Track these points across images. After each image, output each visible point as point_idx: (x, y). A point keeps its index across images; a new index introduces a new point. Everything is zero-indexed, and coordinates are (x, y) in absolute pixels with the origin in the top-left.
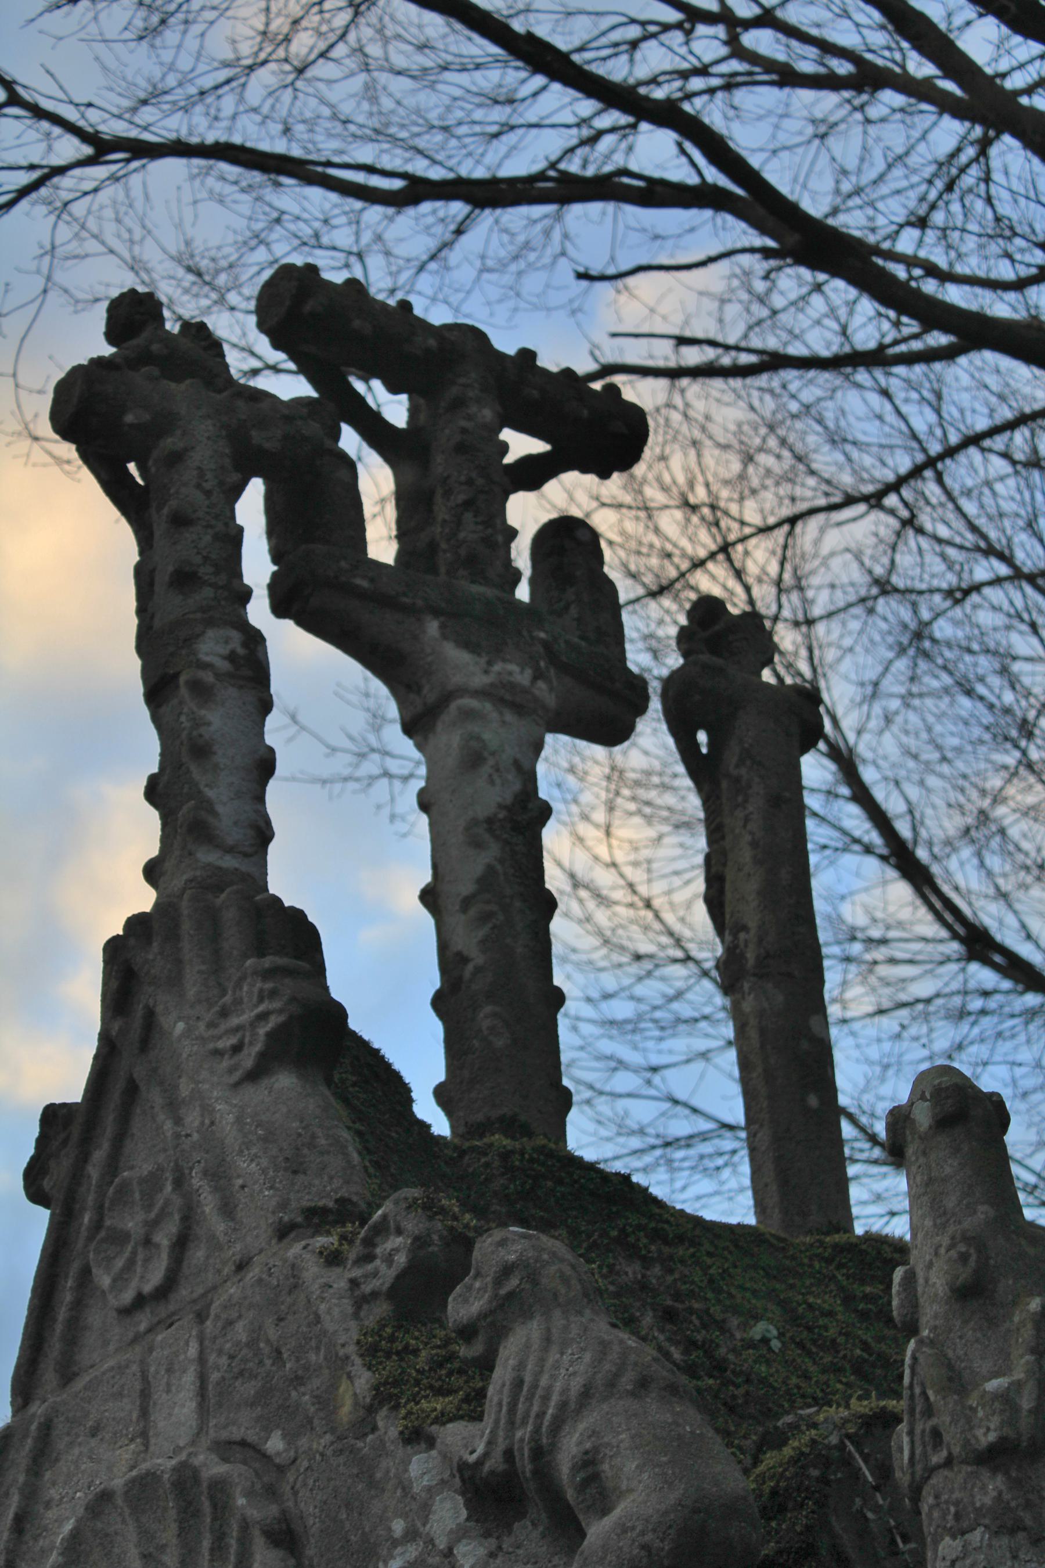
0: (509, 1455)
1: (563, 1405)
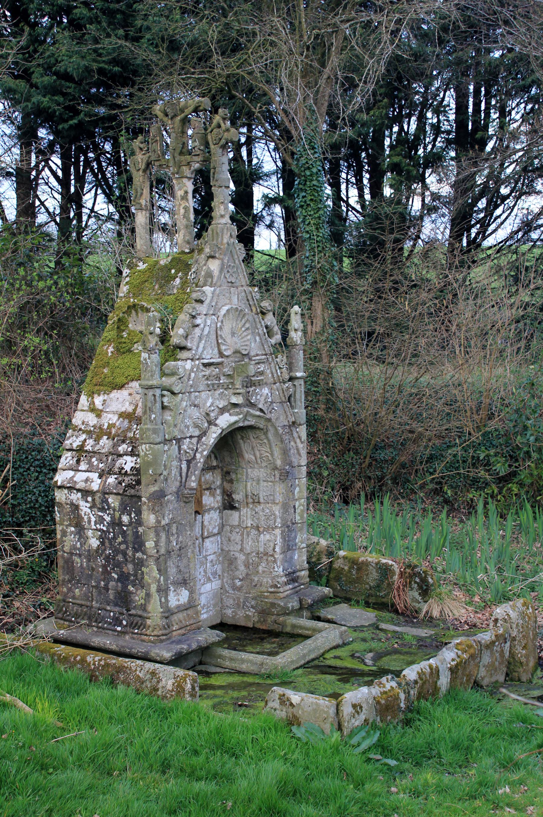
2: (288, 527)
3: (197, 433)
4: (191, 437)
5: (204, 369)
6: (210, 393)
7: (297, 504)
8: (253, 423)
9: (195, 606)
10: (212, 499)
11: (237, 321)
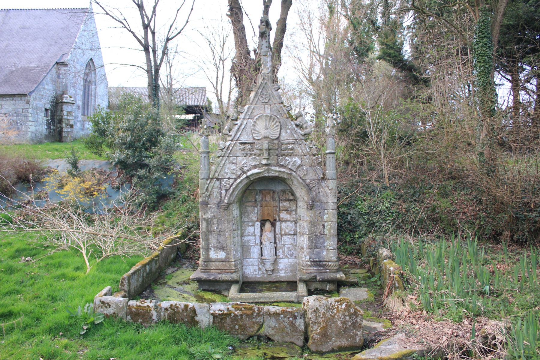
2: (316, 236)
3: (234, 177)
4: (229, 178)
7: (326, 224)
9: (228, 261)
10: (289, 216)
11: (269, 122)
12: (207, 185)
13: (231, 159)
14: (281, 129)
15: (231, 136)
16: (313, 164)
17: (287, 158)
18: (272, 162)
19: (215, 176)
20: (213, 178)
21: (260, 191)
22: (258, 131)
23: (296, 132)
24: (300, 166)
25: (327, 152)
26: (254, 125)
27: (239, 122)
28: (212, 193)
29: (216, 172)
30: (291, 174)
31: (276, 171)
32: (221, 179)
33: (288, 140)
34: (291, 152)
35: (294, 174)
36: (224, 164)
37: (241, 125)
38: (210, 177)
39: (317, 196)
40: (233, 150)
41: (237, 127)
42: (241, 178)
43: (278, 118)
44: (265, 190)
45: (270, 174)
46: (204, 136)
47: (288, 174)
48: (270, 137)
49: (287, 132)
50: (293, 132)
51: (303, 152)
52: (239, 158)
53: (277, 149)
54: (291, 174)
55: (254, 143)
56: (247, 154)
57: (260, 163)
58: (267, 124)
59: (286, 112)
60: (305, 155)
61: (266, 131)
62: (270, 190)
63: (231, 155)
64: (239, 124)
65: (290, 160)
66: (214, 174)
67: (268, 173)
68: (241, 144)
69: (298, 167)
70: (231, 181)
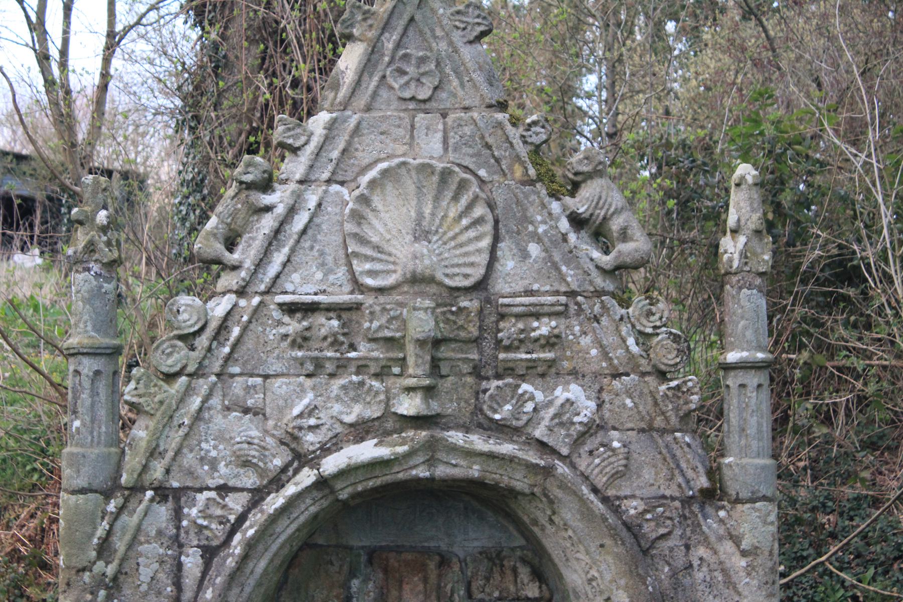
0: (592, 215)
1: (616, 209)
3: (250, 480)
4: (224, 489)
5: (286, 319)
6: (309, 383)
8: (476, 475)
11: (437, 199)
12: (105, 525)
13: (238, 386)
14: (496, 239)
15: (235, 268)
16: (659, 422)
17: (525, 387)
18: (450, 408)
19: (147, 479)
20: (137, 489)
21: (372, 555)
22: (378, 248)
23: (571, 256)
24: (593, 428)
25: (732, 357)
26: (357, 217)
27: (278, 198)
28: (128, 567)
29: (154, 453)
30: (548, 471)
31: (470, 454)
32: (178, 493)
33: (529, 293)
34: (549, 355)
35: (562, 468)
36: (198, 416)
37: (292, 211)
38: (124, 480)
39: (677, 585)
40: (249, 343)
41: (267, 223)
42: (291, 490)
43: (482, 182)
44: (399, 550)
45: (441, 471)
46: (96, 268)
47: (532, 468)
48: (439, 276)
49: (524, 255)
50: (557, 257)
51: (605, 354)
52: (279, 386)
53: (476, 341)
54: (548, 471)
55: (357, 307)
56: (319, 364)
57: (388, 413)
58: (427, 211)
59: (523, 150)
60: (616, 375)
61: (421, 248)
62: (427, 552)
63: (236, 370)
64: (280, 210)
65: (539, 396)
66: (145, 468)
67: (431, 462)
68: (291, 309)
69: (582, 435)
70: (236, 503)
